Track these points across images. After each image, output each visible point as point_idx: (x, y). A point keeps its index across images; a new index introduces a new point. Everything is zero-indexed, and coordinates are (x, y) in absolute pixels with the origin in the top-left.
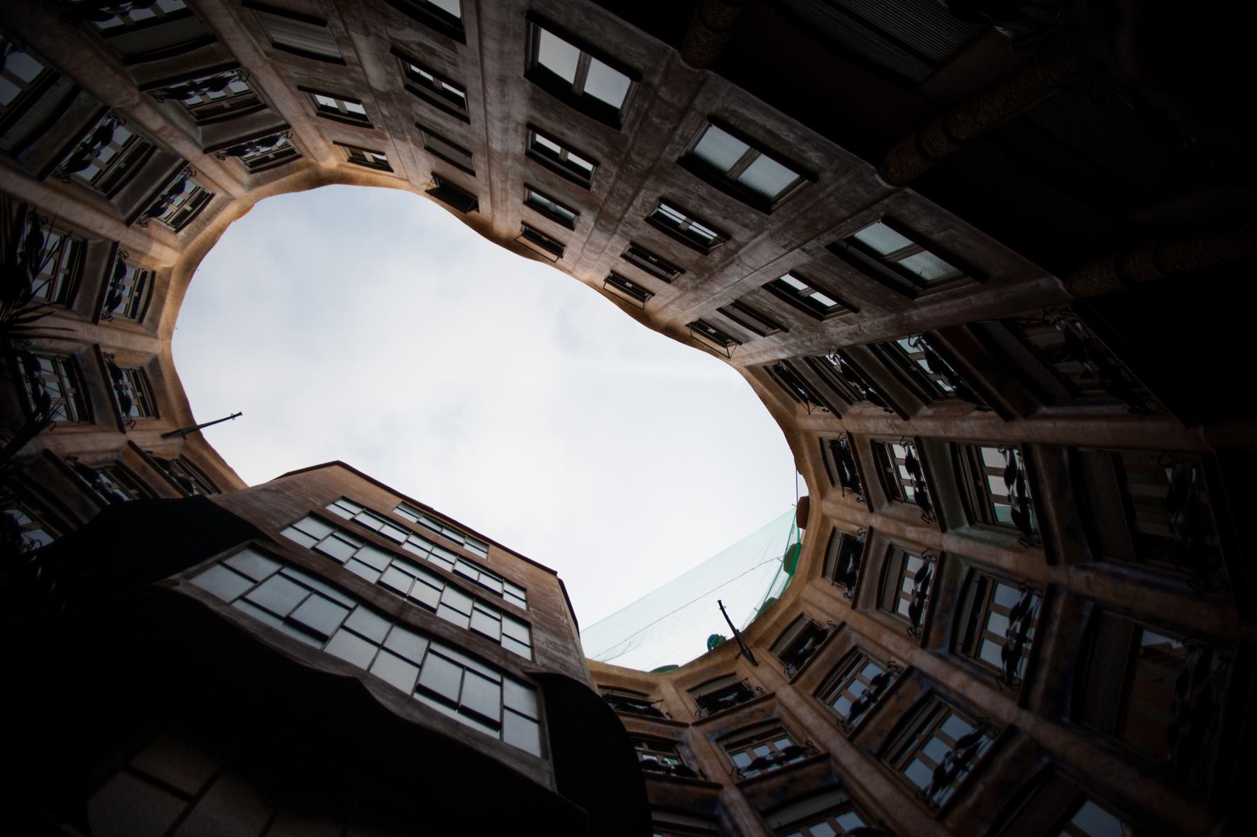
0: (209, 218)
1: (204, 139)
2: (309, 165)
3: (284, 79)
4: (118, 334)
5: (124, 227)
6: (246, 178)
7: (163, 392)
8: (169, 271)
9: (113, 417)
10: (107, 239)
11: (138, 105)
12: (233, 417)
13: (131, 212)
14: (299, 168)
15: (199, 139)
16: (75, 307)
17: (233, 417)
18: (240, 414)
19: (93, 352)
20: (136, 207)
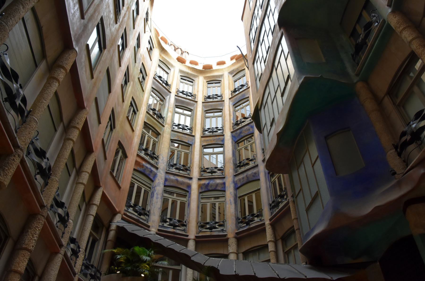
0: (188, 73)
1: (168, 95)
2: (160, 55)
3: (143, 97)
4: (225, 91)
5: (198, 102)
6: (172, 69)
7: (237, 69)
8: (205, 78)
9: (246, 91)
10: (203, 106)
11: (168, 124)
12: (239, 48)
13: (194, 103)
14: (163, 58)
15: (168, 97)
16: (221, 108)
17: (239, 48)
18: (237, 47)
19: (231, 100)
20: (192, 102)
